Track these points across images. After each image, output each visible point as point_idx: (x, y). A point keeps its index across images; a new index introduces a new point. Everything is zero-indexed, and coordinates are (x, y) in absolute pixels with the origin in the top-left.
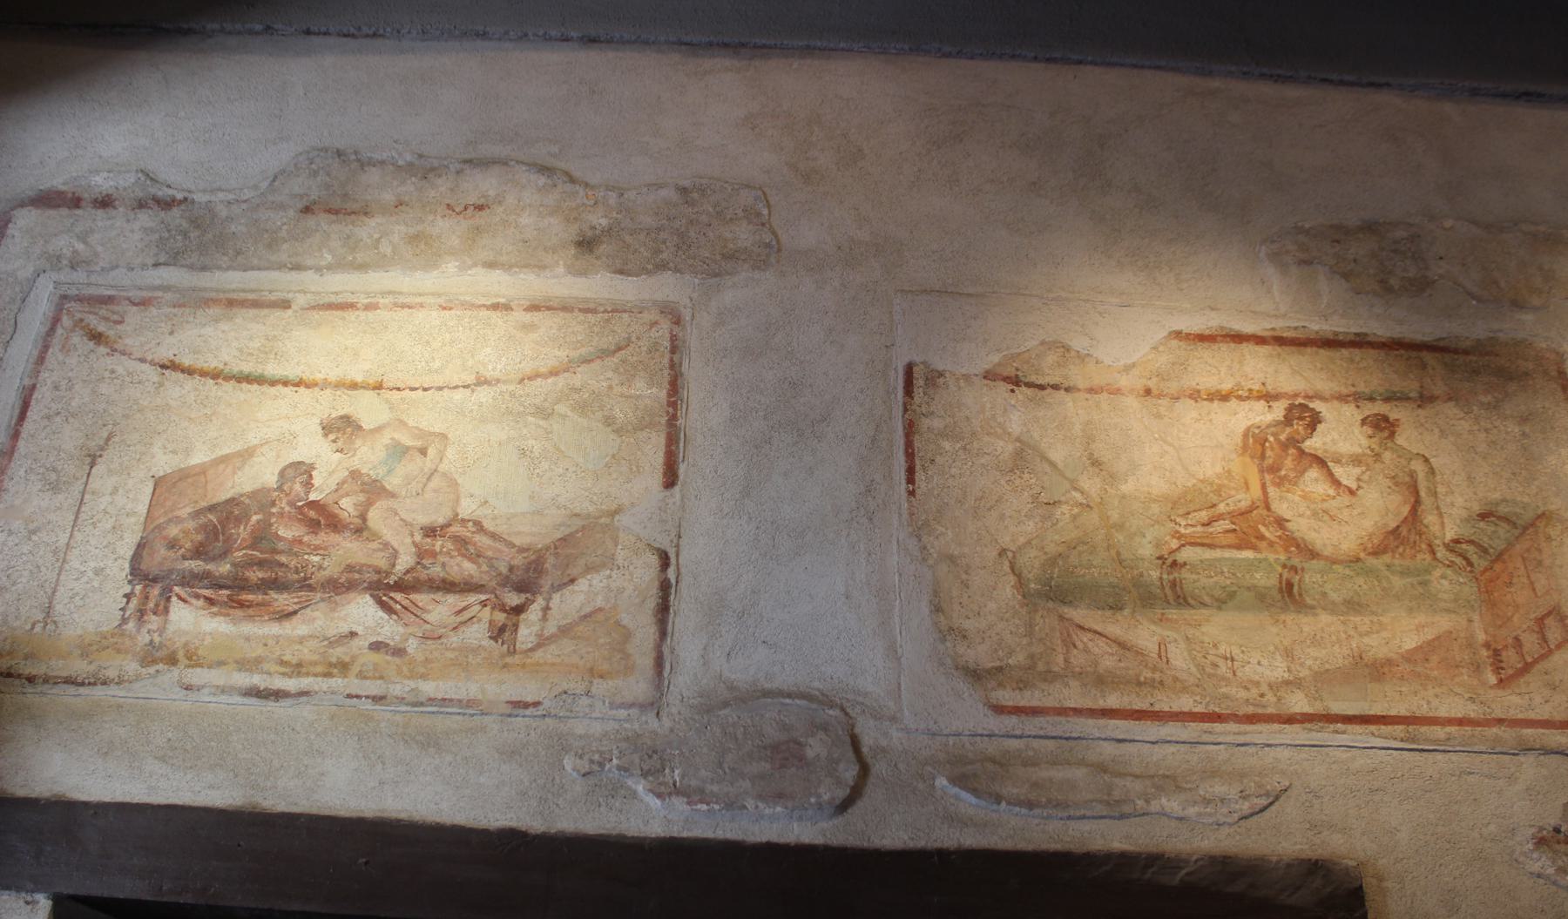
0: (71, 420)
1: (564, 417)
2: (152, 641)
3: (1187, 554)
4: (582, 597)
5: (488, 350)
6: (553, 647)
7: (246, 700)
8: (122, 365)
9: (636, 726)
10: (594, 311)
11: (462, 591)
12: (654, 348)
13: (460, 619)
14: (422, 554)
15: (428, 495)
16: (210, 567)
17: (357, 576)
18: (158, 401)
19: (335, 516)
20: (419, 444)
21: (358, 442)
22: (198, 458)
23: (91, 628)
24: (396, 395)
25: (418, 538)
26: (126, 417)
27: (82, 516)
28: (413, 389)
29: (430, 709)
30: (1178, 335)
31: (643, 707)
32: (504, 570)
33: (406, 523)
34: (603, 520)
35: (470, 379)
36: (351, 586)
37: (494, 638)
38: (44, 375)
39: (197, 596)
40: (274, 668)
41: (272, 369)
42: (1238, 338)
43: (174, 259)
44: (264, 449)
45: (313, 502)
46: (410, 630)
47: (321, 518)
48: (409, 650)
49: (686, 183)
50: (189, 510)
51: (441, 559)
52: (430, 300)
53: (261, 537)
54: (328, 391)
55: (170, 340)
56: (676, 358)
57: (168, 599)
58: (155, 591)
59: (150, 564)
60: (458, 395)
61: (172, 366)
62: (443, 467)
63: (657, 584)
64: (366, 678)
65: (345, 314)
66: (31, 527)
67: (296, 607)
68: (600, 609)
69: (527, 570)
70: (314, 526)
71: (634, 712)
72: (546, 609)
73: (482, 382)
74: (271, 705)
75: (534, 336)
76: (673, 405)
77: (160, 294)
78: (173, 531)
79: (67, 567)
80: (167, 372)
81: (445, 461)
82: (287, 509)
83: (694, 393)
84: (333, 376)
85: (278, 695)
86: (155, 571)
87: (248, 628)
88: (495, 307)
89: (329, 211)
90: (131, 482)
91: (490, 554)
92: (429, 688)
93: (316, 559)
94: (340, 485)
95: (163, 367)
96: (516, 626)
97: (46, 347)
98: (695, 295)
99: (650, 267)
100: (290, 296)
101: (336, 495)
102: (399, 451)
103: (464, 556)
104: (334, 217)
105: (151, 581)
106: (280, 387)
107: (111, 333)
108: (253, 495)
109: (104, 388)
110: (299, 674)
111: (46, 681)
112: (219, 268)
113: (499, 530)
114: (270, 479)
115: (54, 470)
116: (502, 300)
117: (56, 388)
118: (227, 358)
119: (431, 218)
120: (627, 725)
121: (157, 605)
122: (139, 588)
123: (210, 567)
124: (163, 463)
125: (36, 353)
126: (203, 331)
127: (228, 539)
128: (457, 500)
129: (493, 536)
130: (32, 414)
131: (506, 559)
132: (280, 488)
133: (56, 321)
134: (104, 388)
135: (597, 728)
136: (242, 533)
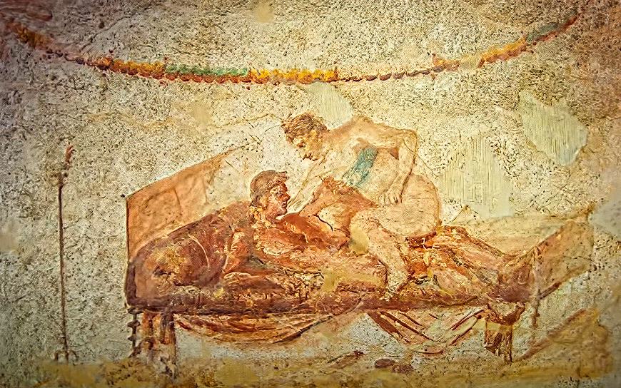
2: (167, 369)
8: (63, 70)
13: (457, 333)
15: (408, 202)
19: (317, 230)
20: (389, 144)
21: (326, 146)
22: (165, 173)
24: (354, 88)
25: (405, 250)
27: (67, 243)
32: (494, 281)
34: (578, 220)
35: (429, 64)
36: (348, 306)
39: (200, 324)
44: (230, 158)
45: (292, 216)
47: (303, 233)
53: (249, 258)
57: (172, 327)
58: (158, 321)
60: (420, 83)
66: (25, 256)
67: (298, 330)
68: (582, 312)
70: (300, 242)
78: (159, 256)
80: (107, 73)
81: (419, 162)
82: (268, 224)
86: (151, 301)
87: (255, 353)
90: (103, 203)
91: (478, 263)
93: (308, 277)
95: (102, 67)
96: (510, 335)
101: (314, 208)
106: (229, 83)
107: (43, 32)
108: (230, 210)
109: (51, 98)
113: (484, 236)
118: (166, 52)
121: (163, 334)
122: (140, 316)
124: (131, 181)
129: (478, 244)
131: (497, 267)
132: (255, 202)
134: (51, 98)
136: (229, 255)
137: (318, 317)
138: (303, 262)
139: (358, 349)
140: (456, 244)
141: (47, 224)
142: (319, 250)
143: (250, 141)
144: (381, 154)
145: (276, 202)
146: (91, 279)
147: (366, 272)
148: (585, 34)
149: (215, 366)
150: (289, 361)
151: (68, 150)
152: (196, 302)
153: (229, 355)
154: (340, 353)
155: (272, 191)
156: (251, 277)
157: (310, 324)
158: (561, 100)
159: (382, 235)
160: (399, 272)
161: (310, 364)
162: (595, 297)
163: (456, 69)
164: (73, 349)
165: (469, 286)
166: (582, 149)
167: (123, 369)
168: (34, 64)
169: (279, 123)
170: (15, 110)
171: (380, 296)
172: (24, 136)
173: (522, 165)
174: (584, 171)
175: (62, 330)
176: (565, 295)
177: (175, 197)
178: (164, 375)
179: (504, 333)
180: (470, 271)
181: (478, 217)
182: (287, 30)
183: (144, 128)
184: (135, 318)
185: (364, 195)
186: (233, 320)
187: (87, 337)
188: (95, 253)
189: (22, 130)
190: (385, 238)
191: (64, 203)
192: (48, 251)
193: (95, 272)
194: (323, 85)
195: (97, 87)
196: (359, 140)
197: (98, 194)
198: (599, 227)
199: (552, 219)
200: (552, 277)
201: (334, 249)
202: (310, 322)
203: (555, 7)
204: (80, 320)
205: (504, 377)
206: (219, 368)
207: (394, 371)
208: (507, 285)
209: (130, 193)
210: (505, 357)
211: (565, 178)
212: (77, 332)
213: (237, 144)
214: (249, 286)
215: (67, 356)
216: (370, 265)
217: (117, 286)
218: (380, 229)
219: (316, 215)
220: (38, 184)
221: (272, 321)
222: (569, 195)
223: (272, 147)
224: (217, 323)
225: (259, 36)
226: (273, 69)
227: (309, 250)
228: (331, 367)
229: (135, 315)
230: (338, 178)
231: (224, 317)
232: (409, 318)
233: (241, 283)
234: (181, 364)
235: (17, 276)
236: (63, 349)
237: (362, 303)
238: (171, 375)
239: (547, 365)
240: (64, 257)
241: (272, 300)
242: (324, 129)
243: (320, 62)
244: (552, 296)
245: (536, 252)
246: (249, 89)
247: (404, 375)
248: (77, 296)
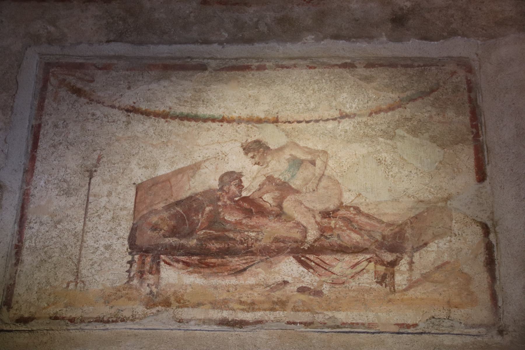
0: (71, 148)
1: (403, 137)
2: (151, 292)
4: (434, 255)
5: (345, 95)
6: (420, 288)
8: (99, 111)
9: (486, 339)
10: (411, 66)
11: (353, 253)
12: (456, 89)
13: (354, 271)
14: (323, 230)
15: (321, 191)
16: (183, 241)
17: (282, 245)
18: (129, 134)
19: (261, 206)
20: (309, 157)
21: (269, 158)
22: (163, 170)
23: (108, 285)
24: (288, 126)
25: (318, 219)
26: (109, 144)
27: (90, 211)
28: (299, 122)
29: (344, 330)
31: (488, 327)
32: (379, 238)
33: (309, 210)
35: (336, 114)
36: (279, 252)
37: (380, 283)
38: (45, 118)
39: (178, 261)
40: (236, 306)
41: (202, 111)
43: (120, 38)
44: (207, 164)
45: (245, 197)
46: (323, 279)
47: (252, 207)
48: (325, 292)
50: (162, 205)
51: (336, 232)
53: (214, 221)
54: (243, 125)
55: (129, 93)
56: (472, 95)
57: (158, 264)
58: (149, 259)
59: (142, 241)
60: (330, 125)
61: (133, 110)
62: (328, 172)
63: (483, 245)
64: (298, 311)
65: (244, 73)
66: (56, 219)
67: (245, 266)
68: (448, 263)
69: (394, 238)
70: (248, 213)
71: (482, 330)
72: (411, 263)
73: (344, 116)
75: (374, 84)
76: (475, 126)
77: (115, 62)
78: (154, 219)
79: (85, 245)
80: (131, 114)
81: (328, 168)
82: (228, 202)
83: (489, 118)
84: (244, 114)
85: (242, 324)
86: (146, 245)
87: (215, 281)
88: (345, 66)
89: (220, 3)
91: (368, 228)
92: (342, 316)
93: (253, 234)
94: (261, 186)
96: (393, 274)
97: (42, 100)
98: (479, 52)
99: (445, 34)
100: (205, 61)
102: (297, 164)
103: (350, 229)
104: (224, 7)
105: (145, 252)
106: (210, 123)
107: (87, 89)
110: (253, 310)
111: (82, 321)
112: (153, 43)
113: (371, 212)
114: (215, 184)
115: (65, 181)
116: (349, 61)
117: (56, 126)
118: (170, 104)
119: (290, 6)
120: (479, 339)
121: (151, 268)
122: (137, 257)
123: (183, 241)
124: (140, 175)
125: (36, 103)
126: (150, 87)
127: (192, 223)
128: (341, 194)
129: (368, 216)
130: (43, 144)
132: (221, 189)
133: (46, 81)
134: (90, 126)
135: (458, 341)
136: (201, 219)
137: (259, 258)
138: (250, 225)
139: (285, 279)
140: (353, 216)
141: (77, 200)
142: (261, 218)
143: (220, 154)
144: (305, 164)
145: (235, 189)
146: (104, 234)
147: (292, 231)
148: (444, 97)
149: (186, 290)
150: (238, 287)
151: (99, 156)
152: (177, 248)
153: (196, 282)
154: (273, 281)
155: (232, 183)
156: (216, 233)
157: (253, 263)
158: (425, 134)
159: (303, 210)
160: (315, 232)
161: (252, 289)
162: (456, 254)
163: (354, 117)
164: (83, 279)
165: (362, 241)
166: (440, 162)
167: (118, 293)
168: (79, 106)
169: (240, 145)
170: (63, 132)
171: (302, 245)
172: (67, 147)
173: (397, 170)
174: (443, 175)
175: (76, 266)
176: (433, 251)
177: (169, 185)
178: (148, 296)
179: (389, 273)
180: (363, 232)
181: (367, 201)
182: (248, 96)
183: (152, 145)
184: (133, 258)
185: (293, 186)
186: (200, 260)
187: (95, 271)
188: (109, 217)
189: (66, 143)
190: (306, 212)
191: (92, 187)
192: (75, 216)
193: (109, 229)
194: (269, 125)
195: (124, 122)
196: (291, 155)
197: (117, 182)
198: (456, 209)
199: (421, 203)
200: (422, 239)
201: (271, 218)
202: (253, 261)
203: (423, 82)
204: (91, 260)
205: (390, 303)
206: (188, 291)
207: (310, 294)
208: (389, 242)
209: (140, 182)
210: (390, 289)
211: (428, 179)
212: (88, 267)
213: (211, 156)
214: (214, 239)
215: (76, 285)
216: (294, 227)
217: (123, 238)
218: (303, 206)
219: (261, 198)
220: (75, 176)
221: (228, 261)
222: (432, 190)
223: (234, 157)
224: (190, 261)
225: (230, 98)
226: (238, 116)
227: (255, 218)
228: (267, 291)
229: (133, 256)
230: (276, 176)
231: (195, 257)
232: (321, 260)
233: (209, 237)
234: (162, 288)
235: (47, 232)
236: (75, 279)
237: (289, 250)
238: (153, 295)
239: (423, 297)
240: (87, 220)
241: (228, 248)
242: (268, 148)
243: (268, 113)
244: (423, 251)
245: (409, 222)
246: (222, 126)
247: (317, 298)
248: (92, 244)
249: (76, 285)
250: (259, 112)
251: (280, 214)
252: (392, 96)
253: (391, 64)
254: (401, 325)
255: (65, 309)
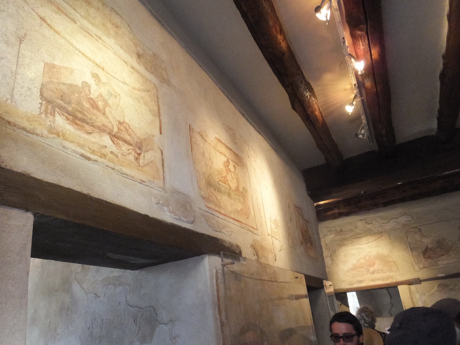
0: (10, 18)
2: (51, 125)
3: (220, 182)
7: (81, 157)
20: (114, 94)
25: (118, 124)
30: (216, 137)
35: (123, 81)
36: (104, 131)
39: (63, 115)
40: (88, 149)
42: (222, 142)
49: (155, 53)
52: (111, 49)
53: (79, 103)
58: (50, 107)
60: (121, 84)
67: (91, 132)
72: (144, 156)
73: (125, 83)
74: (87, 162)
80: (43, 21)
85: (89, 159)
87: (79, 133)
92: (125, 170)
93: (94, 118)
113: (134, 130)
121: (51, 112)
122: (44, 102)
128: (124, 117)
129: (132, 131)
132: (82, 88)
135: (156, 192)
204: (20, 91)
212: (18, 95)
249: (12, 102)
250: (98, 61)
251: (104, 114)
252: (138, 86)
253: (138, 72)
254: (142, 180)
255: (4, 114)
